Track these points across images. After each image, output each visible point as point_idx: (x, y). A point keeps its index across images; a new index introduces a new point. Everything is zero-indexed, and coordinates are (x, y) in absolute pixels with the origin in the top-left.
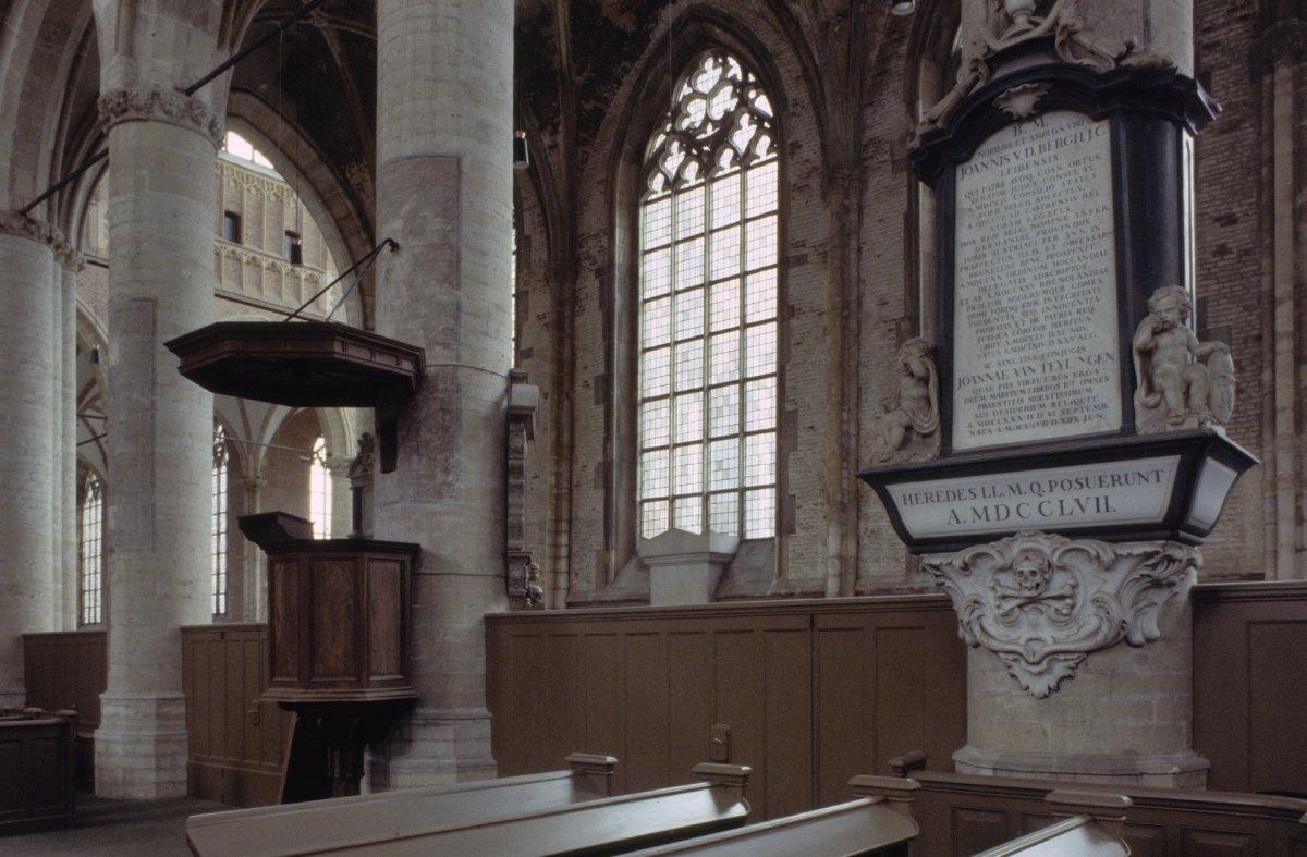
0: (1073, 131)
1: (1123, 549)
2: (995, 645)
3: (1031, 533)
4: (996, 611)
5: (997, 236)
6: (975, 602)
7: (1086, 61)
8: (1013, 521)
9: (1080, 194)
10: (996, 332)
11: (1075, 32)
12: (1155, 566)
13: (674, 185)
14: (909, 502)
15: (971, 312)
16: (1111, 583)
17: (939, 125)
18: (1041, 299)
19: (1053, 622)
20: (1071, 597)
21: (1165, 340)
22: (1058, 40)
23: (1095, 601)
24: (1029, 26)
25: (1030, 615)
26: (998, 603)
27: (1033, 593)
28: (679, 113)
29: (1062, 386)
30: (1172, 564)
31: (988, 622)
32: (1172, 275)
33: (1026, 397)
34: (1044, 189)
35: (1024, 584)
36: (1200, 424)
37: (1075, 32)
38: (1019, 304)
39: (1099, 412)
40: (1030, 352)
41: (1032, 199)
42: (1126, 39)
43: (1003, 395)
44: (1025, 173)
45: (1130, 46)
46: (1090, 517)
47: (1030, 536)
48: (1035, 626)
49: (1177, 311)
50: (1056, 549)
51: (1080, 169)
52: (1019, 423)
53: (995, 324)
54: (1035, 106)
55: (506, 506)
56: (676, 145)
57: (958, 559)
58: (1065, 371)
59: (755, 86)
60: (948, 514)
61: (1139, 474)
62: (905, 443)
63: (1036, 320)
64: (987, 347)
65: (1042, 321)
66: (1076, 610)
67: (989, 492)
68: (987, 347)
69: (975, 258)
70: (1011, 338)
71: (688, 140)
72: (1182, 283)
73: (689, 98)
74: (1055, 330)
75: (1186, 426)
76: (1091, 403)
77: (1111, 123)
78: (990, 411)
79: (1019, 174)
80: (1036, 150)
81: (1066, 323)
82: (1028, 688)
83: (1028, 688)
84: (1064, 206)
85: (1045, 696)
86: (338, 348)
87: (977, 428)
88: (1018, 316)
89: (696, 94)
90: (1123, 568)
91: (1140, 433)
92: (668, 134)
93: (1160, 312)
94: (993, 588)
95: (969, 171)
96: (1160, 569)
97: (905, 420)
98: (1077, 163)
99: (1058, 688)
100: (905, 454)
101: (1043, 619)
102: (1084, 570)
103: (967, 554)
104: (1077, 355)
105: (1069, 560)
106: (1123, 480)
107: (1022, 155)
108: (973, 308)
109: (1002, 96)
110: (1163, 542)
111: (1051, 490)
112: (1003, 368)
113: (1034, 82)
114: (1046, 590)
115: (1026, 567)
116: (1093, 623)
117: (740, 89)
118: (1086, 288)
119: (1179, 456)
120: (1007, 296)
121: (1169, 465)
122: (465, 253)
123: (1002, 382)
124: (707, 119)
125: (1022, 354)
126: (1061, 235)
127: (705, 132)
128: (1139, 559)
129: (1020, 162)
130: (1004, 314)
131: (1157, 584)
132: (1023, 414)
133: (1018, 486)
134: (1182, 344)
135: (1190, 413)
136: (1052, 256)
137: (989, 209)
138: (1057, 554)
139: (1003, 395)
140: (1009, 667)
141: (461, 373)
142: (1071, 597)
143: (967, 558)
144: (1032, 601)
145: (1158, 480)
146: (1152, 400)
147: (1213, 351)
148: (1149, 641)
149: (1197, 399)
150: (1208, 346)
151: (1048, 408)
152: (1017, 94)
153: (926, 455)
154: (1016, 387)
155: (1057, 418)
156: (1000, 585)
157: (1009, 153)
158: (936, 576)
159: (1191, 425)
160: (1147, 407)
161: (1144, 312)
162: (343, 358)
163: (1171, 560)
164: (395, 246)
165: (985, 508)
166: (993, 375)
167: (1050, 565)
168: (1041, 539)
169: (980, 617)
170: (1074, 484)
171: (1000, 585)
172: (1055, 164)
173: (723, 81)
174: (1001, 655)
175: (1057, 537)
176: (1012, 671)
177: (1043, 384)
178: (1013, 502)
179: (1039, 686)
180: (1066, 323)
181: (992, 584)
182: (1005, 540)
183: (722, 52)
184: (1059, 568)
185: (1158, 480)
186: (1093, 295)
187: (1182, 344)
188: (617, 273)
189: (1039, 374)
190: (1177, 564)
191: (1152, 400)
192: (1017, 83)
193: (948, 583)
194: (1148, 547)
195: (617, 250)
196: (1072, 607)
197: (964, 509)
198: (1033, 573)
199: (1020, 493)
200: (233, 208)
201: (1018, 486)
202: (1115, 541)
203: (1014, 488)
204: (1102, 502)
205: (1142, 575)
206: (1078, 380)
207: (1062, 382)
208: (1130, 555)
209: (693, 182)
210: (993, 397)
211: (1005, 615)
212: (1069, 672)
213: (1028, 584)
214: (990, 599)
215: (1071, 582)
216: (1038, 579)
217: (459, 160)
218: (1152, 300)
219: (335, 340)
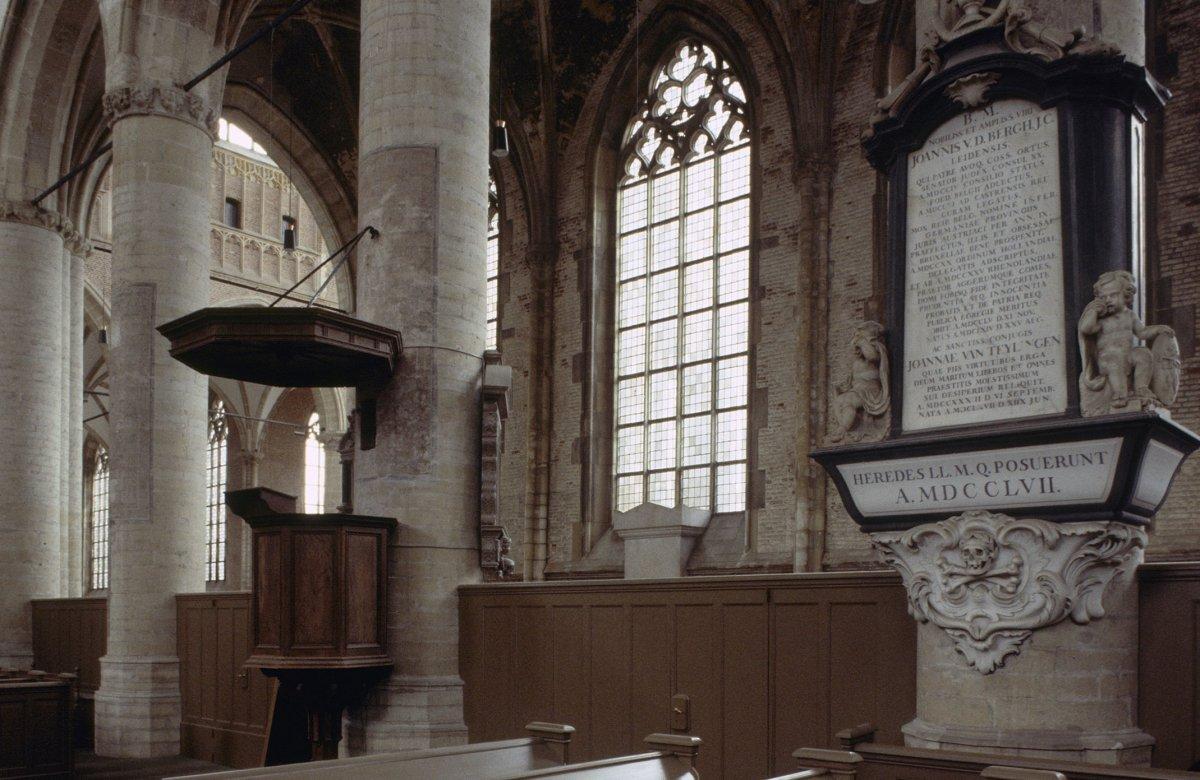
0: (1021, 119)
1: (1067, 529)
2: (941, 621)
3: (978, 513)
4: (943, 588)
5: (947, 222)
6: (923, 579)
7: (1034, 51)
8: (961, 501)
9: (1027, 182)
10: (944, 317)
11: (1024, 22)
12: (1098, 546)
13: (650, 170)
14: (859, 482)
15: (921, 297)
16: (1056, 562)
17: (891, 114)
18: (989, 283)
19: (999, 599)
20: (1016, 575)
21: (1110, 324)
22: (1007, 32)
23: (1040, 579)
24: (979, 17)
25: (976, 592)
26: (944, 581)
27: (979, 571)
28: (655, 100)
29: (1009, 369)
30: (1116, 544)
31: (936, 599)
32: (1120, 259)
33: (973, 381)
34: (993, 176)
35: (970, 563)
36: (1143, 406)
37: (1024, 22)
38: (968, 288)
39: (1045, 394)
40: (976, 336)
41: (982, 185)
42: (1075, 28)
43: (952, 378)
44: (974, 160)
45: (1078, 35)
46: (1035, 497)
47: (976, 515)
48: (981, 603)
49: (1121, 296)
50: (1000, 530)
51: (1028, 156)
52: (966, 405)
53: (944, 308)
54: (985, 95)
55: (479, 483)
56: (652, 131)
57: (906, 537)
58: (1012, 354)
59: (729, 73)
60: (897, 493)
61: (1083, 456)
62: (856, 424)
63: (984, 305)
64: (937, 330)
65: (990, 306)
66: (1021, 588)
67: (936, 472)
68: (937, 330)
69: (926, 243)
70: (960, 322)
71: (664, 126)
72: (1129, 268)
73: (665, 86)
74: (1002, 314)
75: (1128, 409)
76: (1038, 386)
77: (1059, 111)
78: (939, 393)
79: (968, 162)
80: (986, 139)
81: (1014, 307)
82: (973, 664)
83: (973, 664)
84: (1012, 193)
85: (991, 672)
86: (318, 332)
87: (925, 410)
88: (967, 299)
89: (672, 82)
90: (1067, 549)
91: (1086, 415)
92: (644, 121)
93: (1105, 297)
94: (940, 566)
95: (920, 159)
96: (1104, 549)
97: (856, 401)
98: (1026, 150)
99: (1003, 665)
100: (856, 435)
101: (988, 597)
102: (1029, 549)
103: (915, 533)
104: (1024, 338)
105: (1013, 539)
106: (1067, 462)
107: (972, 143)
108: (923, 292)
109: (951, 86)
110: (1107, 522)
111: (997, 471)
112: (952, 351)
113: (981, 72)
114: (992, 568)
115: (972, 546)
116: (1038, 601)
117: (715, 76)
118: (1033, 273)
119: (1122, 439)
120: (956, 281)
121: (1112, 447)
122: (441, 238)
123: (950, 365)
124: (682, 106)
125: (970, 338)
126: (1009, 220)
127: (680, 119)
128: (1082, 539)
129: (970, 150)
130: (953, 298)
131: (1101, 563)
132: (971, 396)
133: (964, 466)
134: (1127, 328)
135: (1134, 395)
136: (1000, 242)
137: (940, 196)
138: (1003, 533)
139: (952, 378)
140: (956, 643)
141: (437, 354)
142: (1016, 575)
143: (915, 537)
144: (978, 579)
145: (1102, 462)
146: (1097, 383)
147: (1158, 334)
148: (1094, 619)
149: (1141, 383)
150: (1154, 330)
151: (996, 390)
152: (967, 84)
153: (877, 436)
154: (965, 370)
155: (1004, 399)
156: (947, 563)
157: (959, 141)
158: (887, 554)
159: (1134, 407)
160: (1090, 389)
161: (1090, 296)
162: (323, 341)
163: (1115, 540)
164: (375, 234)
165: (933, 488)
166: (943, 358)
167: (995, 545)
168: (987, 518)
169: (927, 594)
170: (1020, 465)
171: (947, 563)
172: (1003, 152)
173: (698, 69)
174: (948, 631)
175: (1002, 517)
176: (958, 647)
177: (991, 367)
178: (959, 482)
179: (985, 662)
180: (1014, 307)
181: (939, 562)
182: (952, 519)
183: (696, 42)
184: (1004, 547)
185: (1102, 462)
186: (1040, 281)
187: (1127, 328)
188: (594, 255)
189: (987, 357)
190: (1121, 544)
191: (1097, 383)
192: (965, 73)
193: (897, 561)
194: (1092, 528)
195: (595, 232)
196: (1018, 585)
197: (912, 489)
198: (979, 552)
199: (967, 474)
200: (234, 195)
201: (964, 466)
202: (1059, 521)
203: (961, 468)
204: (1047, 482)
205: (1086, 555)
206: (1025, 362)
207: (1009, 365)
208: (1073, 534)
209: (668, 167)
210: (942, 379)
211: (952, 593)
212: (1015, 649)
213: (974, 563)
214: (937, 576)
215: (1016, 560)
216: (984, 557)
217: (436, 150)
218: (1097, 285)
219: (315, 324)
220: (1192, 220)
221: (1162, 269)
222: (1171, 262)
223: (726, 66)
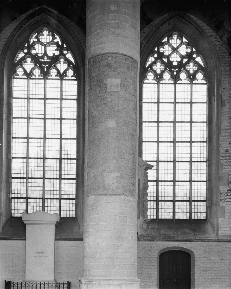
28: (31, 47)
71: (36, 59)
117: (60, 48)
220: (228, 148)
221: (221, 160)
222: (223, 159)
223: (65, 46)
